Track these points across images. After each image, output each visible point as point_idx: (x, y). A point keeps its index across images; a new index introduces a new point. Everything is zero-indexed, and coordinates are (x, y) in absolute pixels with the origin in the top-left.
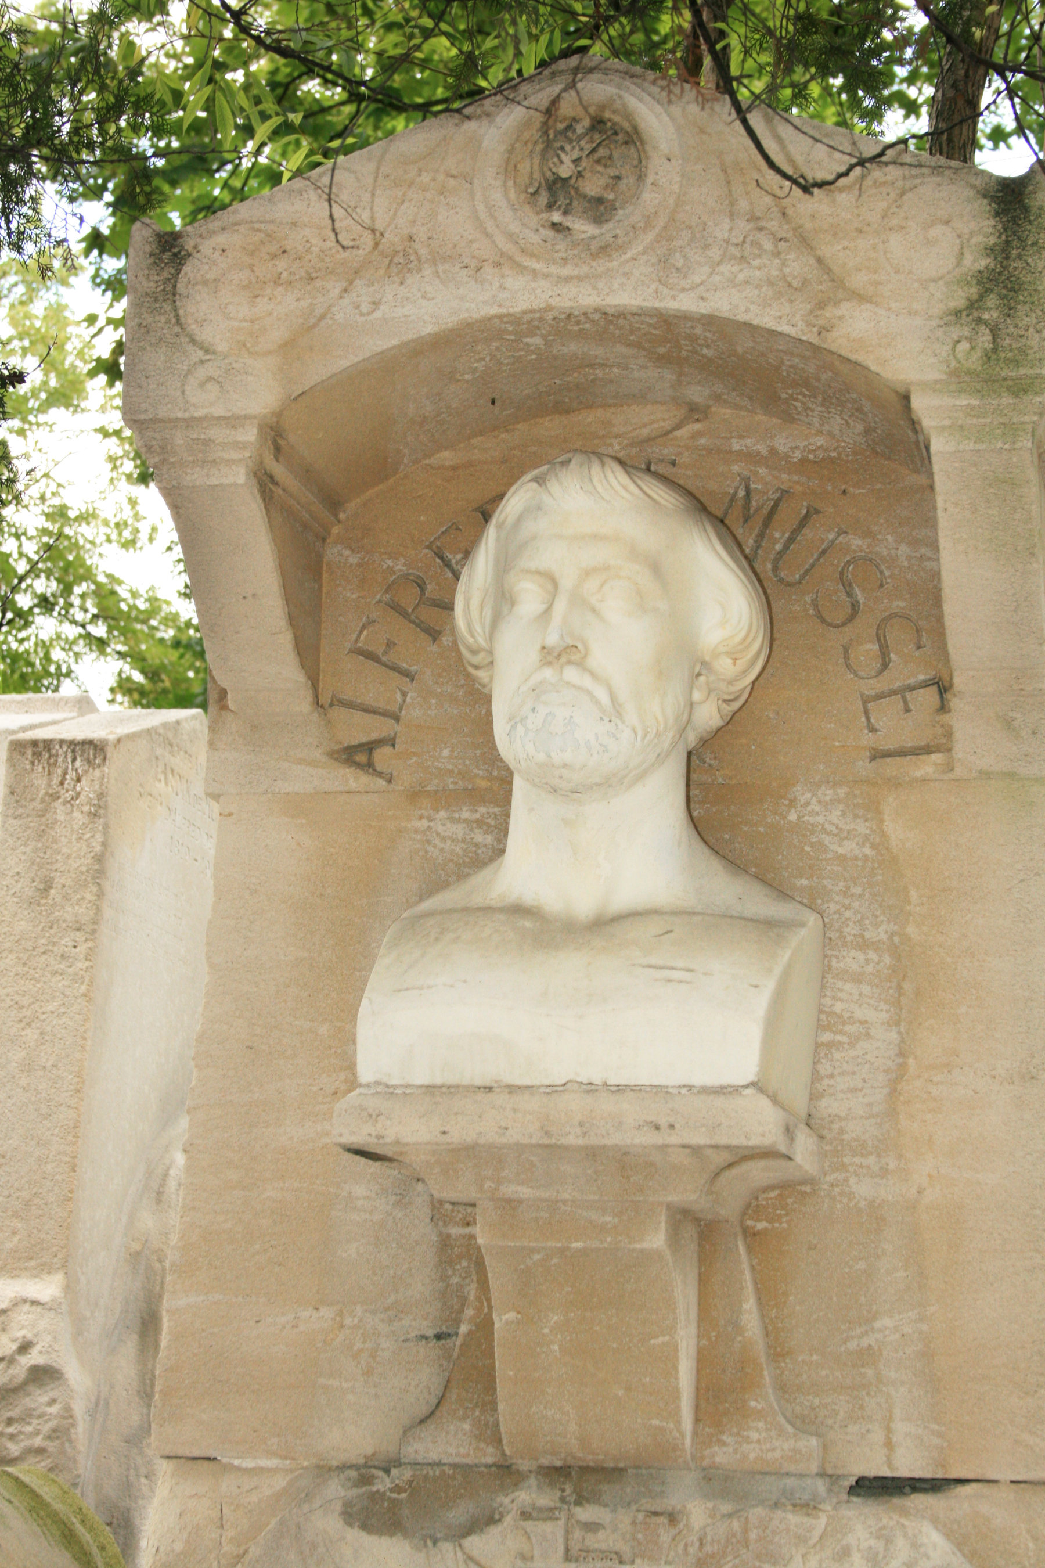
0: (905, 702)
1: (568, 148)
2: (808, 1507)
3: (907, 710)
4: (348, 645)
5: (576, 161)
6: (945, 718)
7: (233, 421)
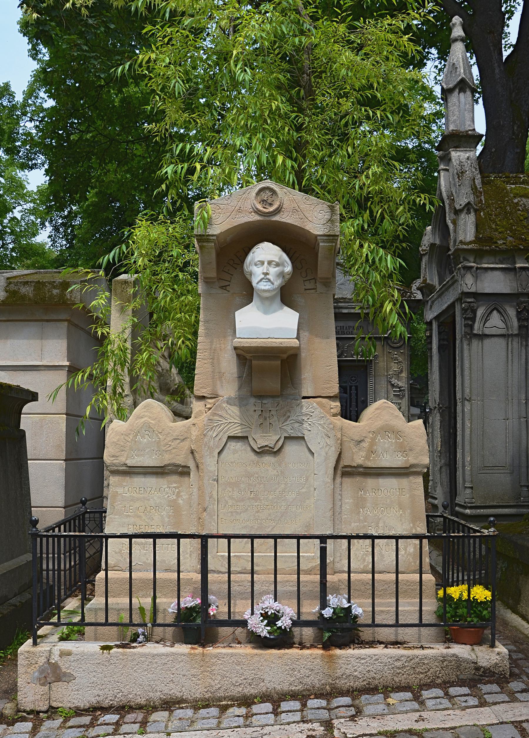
7: (213, 235)
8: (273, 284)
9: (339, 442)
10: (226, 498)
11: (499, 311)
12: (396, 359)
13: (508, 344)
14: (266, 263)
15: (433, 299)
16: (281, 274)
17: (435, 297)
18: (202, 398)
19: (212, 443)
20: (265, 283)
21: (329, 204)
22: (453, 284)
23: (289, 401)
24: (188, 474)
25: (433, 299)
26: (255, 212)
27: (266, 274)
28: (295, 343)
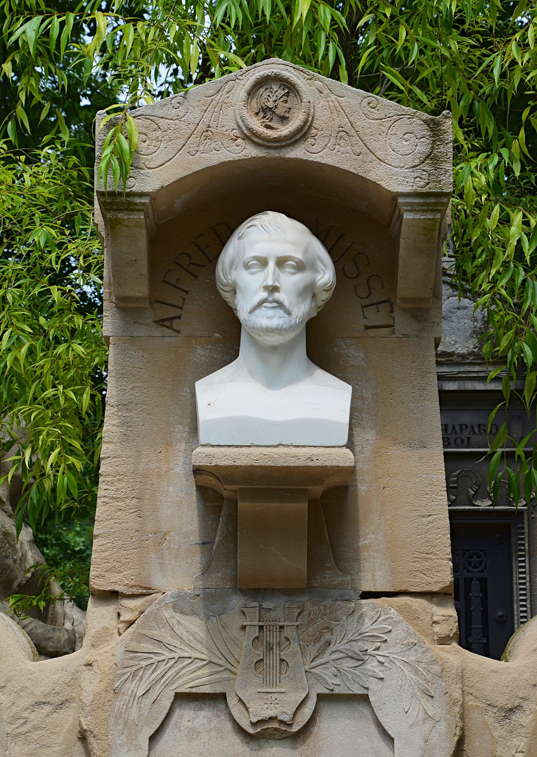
0: (378, 308)
1: (271, 95)
3: (378, 311)
4: (162, 279)
5: (275, 101)
6: (391, 314)
7: (142, 195)
8: (289, 313)
9: (457, 709)
14: (272, 264)
16: (309, 291)
18: (112, 596)
20: (270, 312)
21: (426, 116)
23: (328, 602)
26: (246, 138)
27: (274, 289)
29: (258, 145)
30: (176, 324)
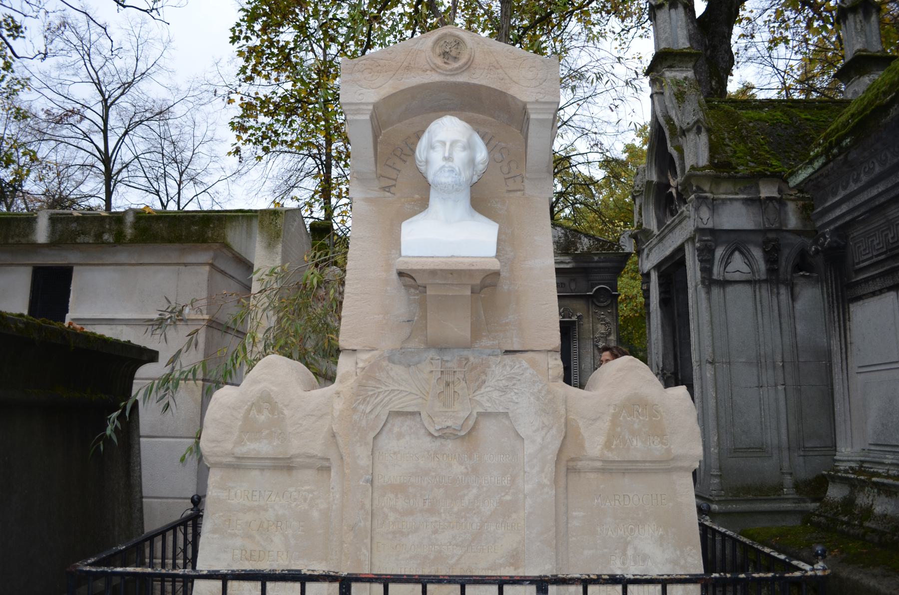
2: (497, 356)
7: (367, 104)
10: (386, 510)
11: (741, 253)
12: (603, 320)
13: (755, 291)
15: (651, 246)
16: (472, 162)
17: (654, 243)
19: (364, 423)
22: (680, 222)
24: (328, 469)
25: (651, 246)
28: (496, 265)
29: (440, 73)
30: (392, 189)
